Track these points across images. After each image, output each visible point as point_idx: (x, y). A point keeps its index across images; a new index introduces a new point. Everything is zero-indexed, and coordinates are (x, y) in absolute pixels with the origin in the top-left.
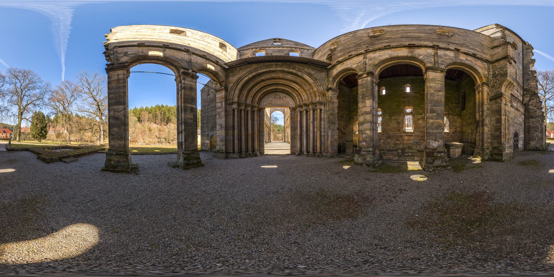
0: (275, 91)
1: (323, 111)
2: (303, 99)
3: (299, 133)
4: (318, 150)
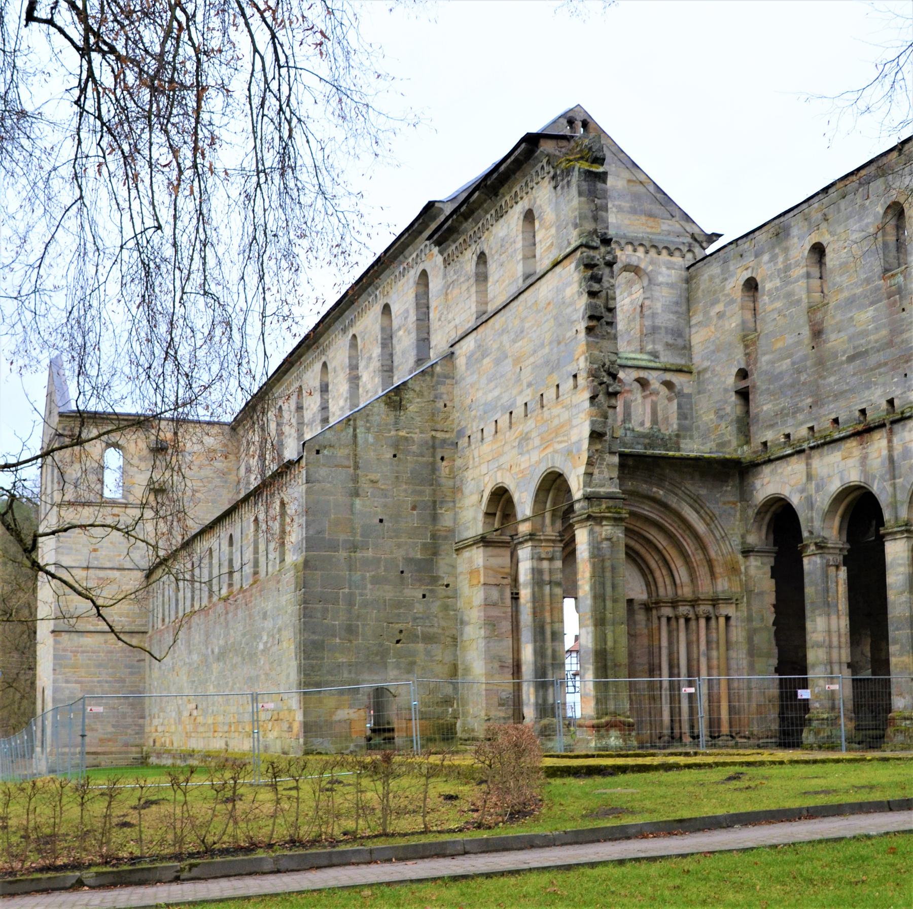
1: (733, 622)
2: (678, 581)
4: (725, 729)
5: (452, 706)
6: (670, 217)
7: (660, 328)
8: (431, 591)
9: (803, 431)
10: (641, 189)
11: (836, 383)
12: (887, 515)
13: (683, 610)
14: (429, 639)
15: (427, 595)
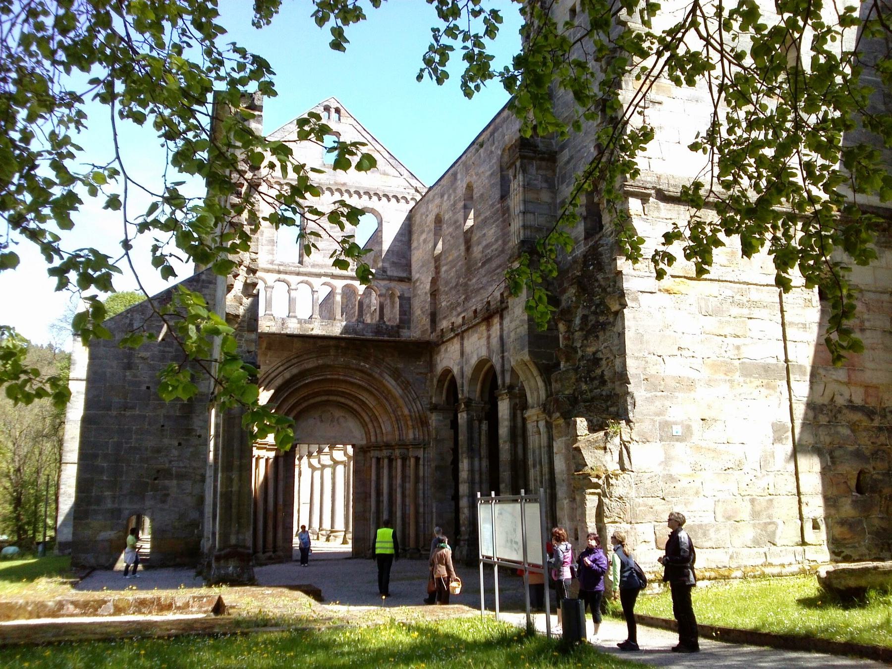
0: (327, 403)
1: (421, 462)
3: (373, 508)
5: (198, 528)
8: (187, 440)
9: (460, 320)
11: (476, 283)
12: (500, 382)
13: (385, 453)
14: (181, 476)
15: (183, 442)
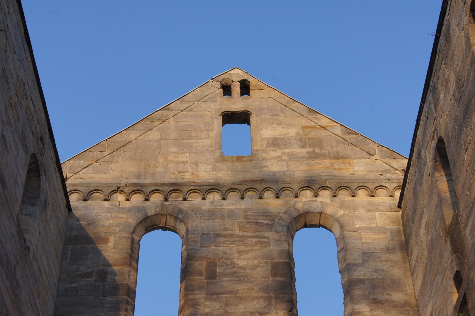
6: (366, 155)
7: (362, 281)
10: (323, 133)
